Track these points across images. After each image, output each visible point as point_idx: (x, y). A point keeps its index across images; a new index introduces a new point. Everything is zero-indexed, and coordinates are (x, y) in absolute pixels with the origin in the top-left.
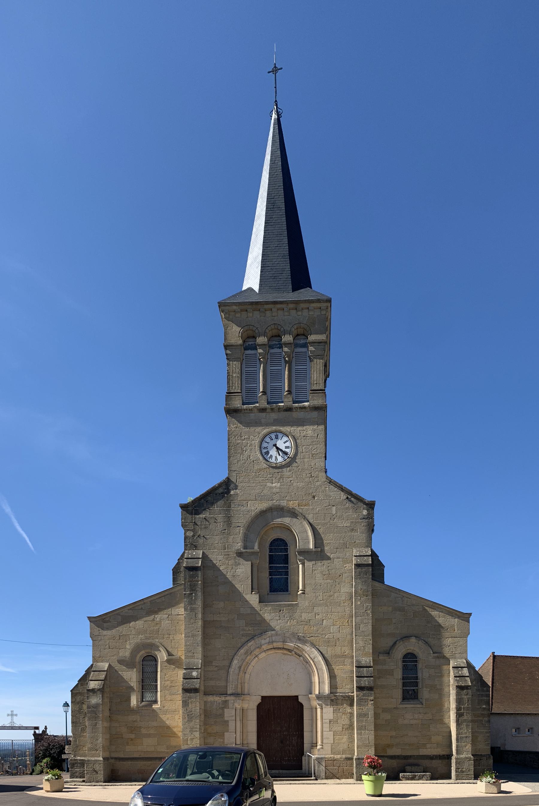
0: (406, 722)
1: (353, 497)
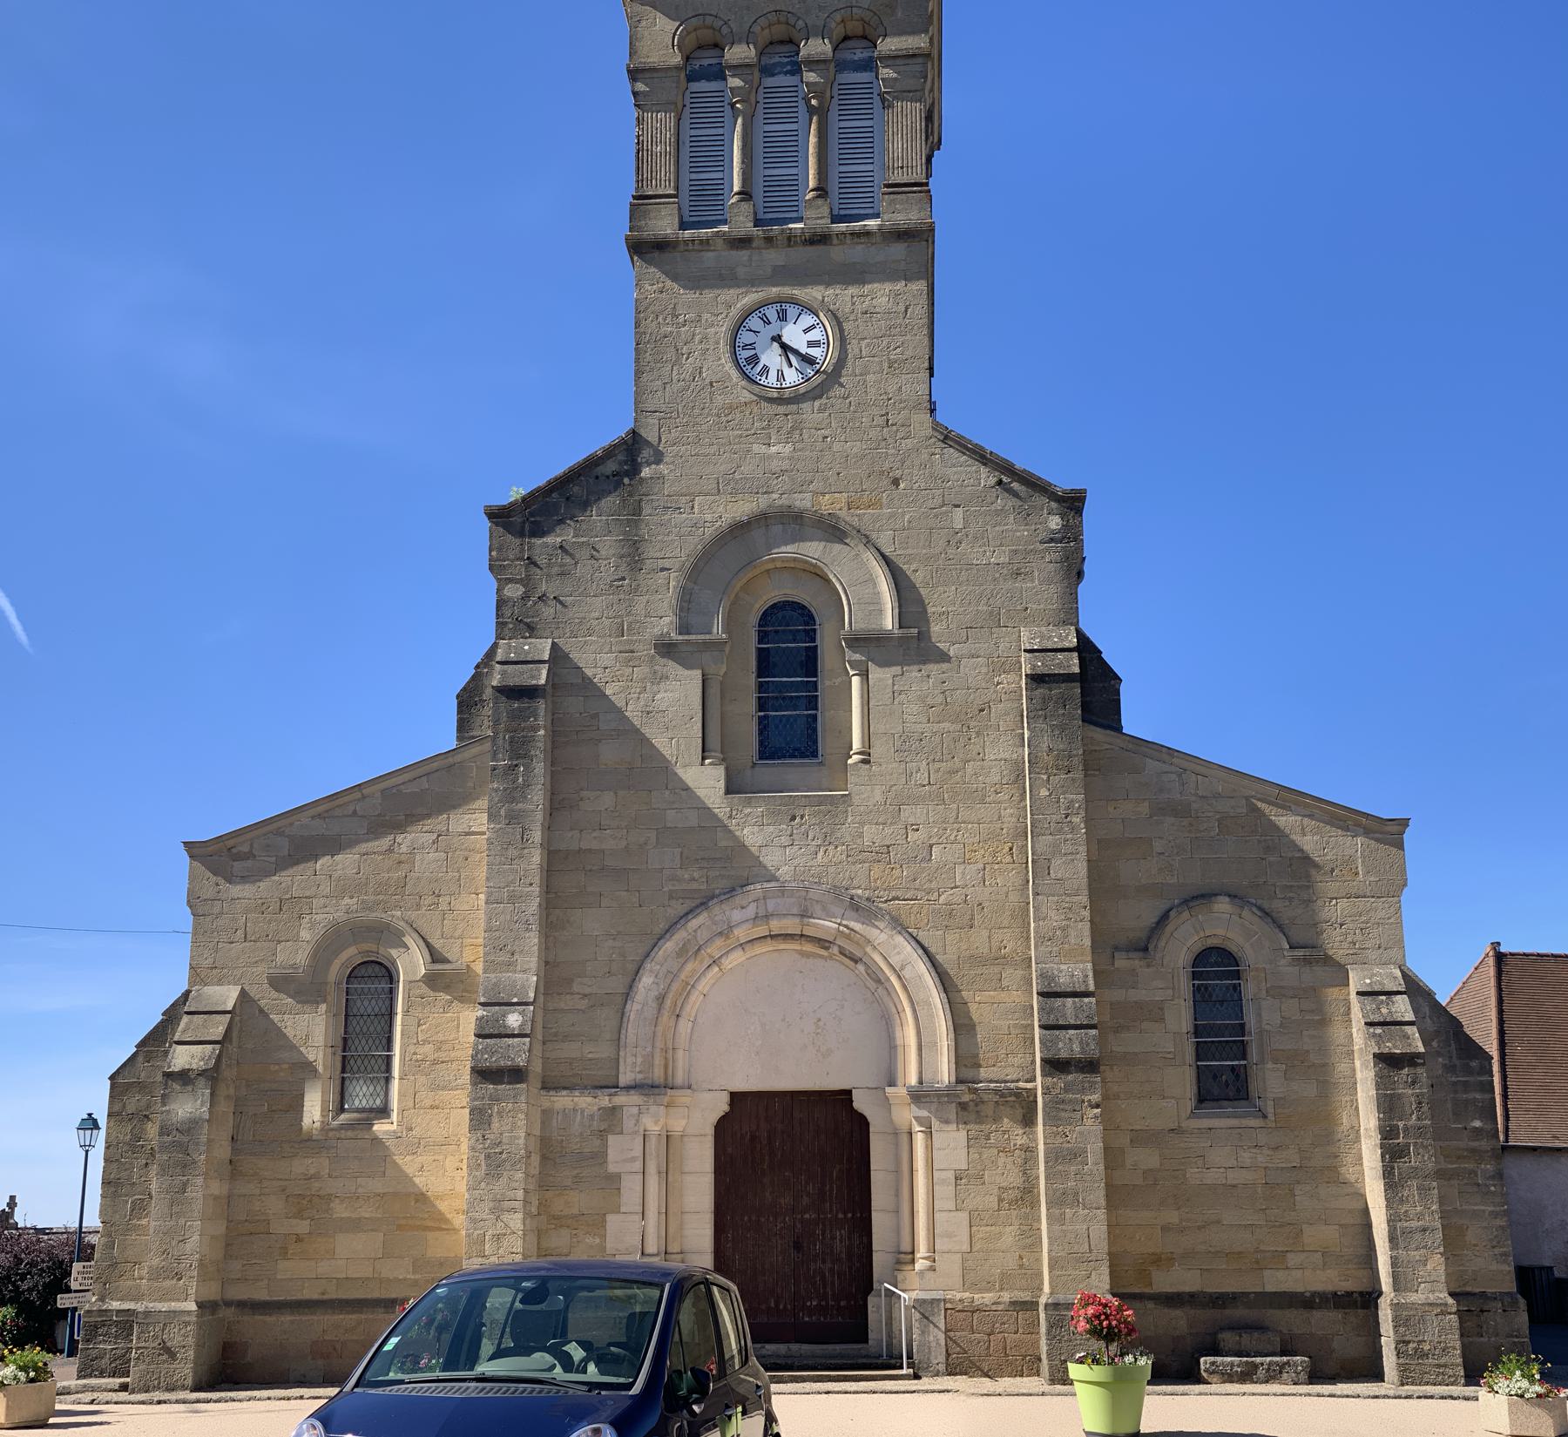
0: (1212, 1177)
1: (1017, 481)
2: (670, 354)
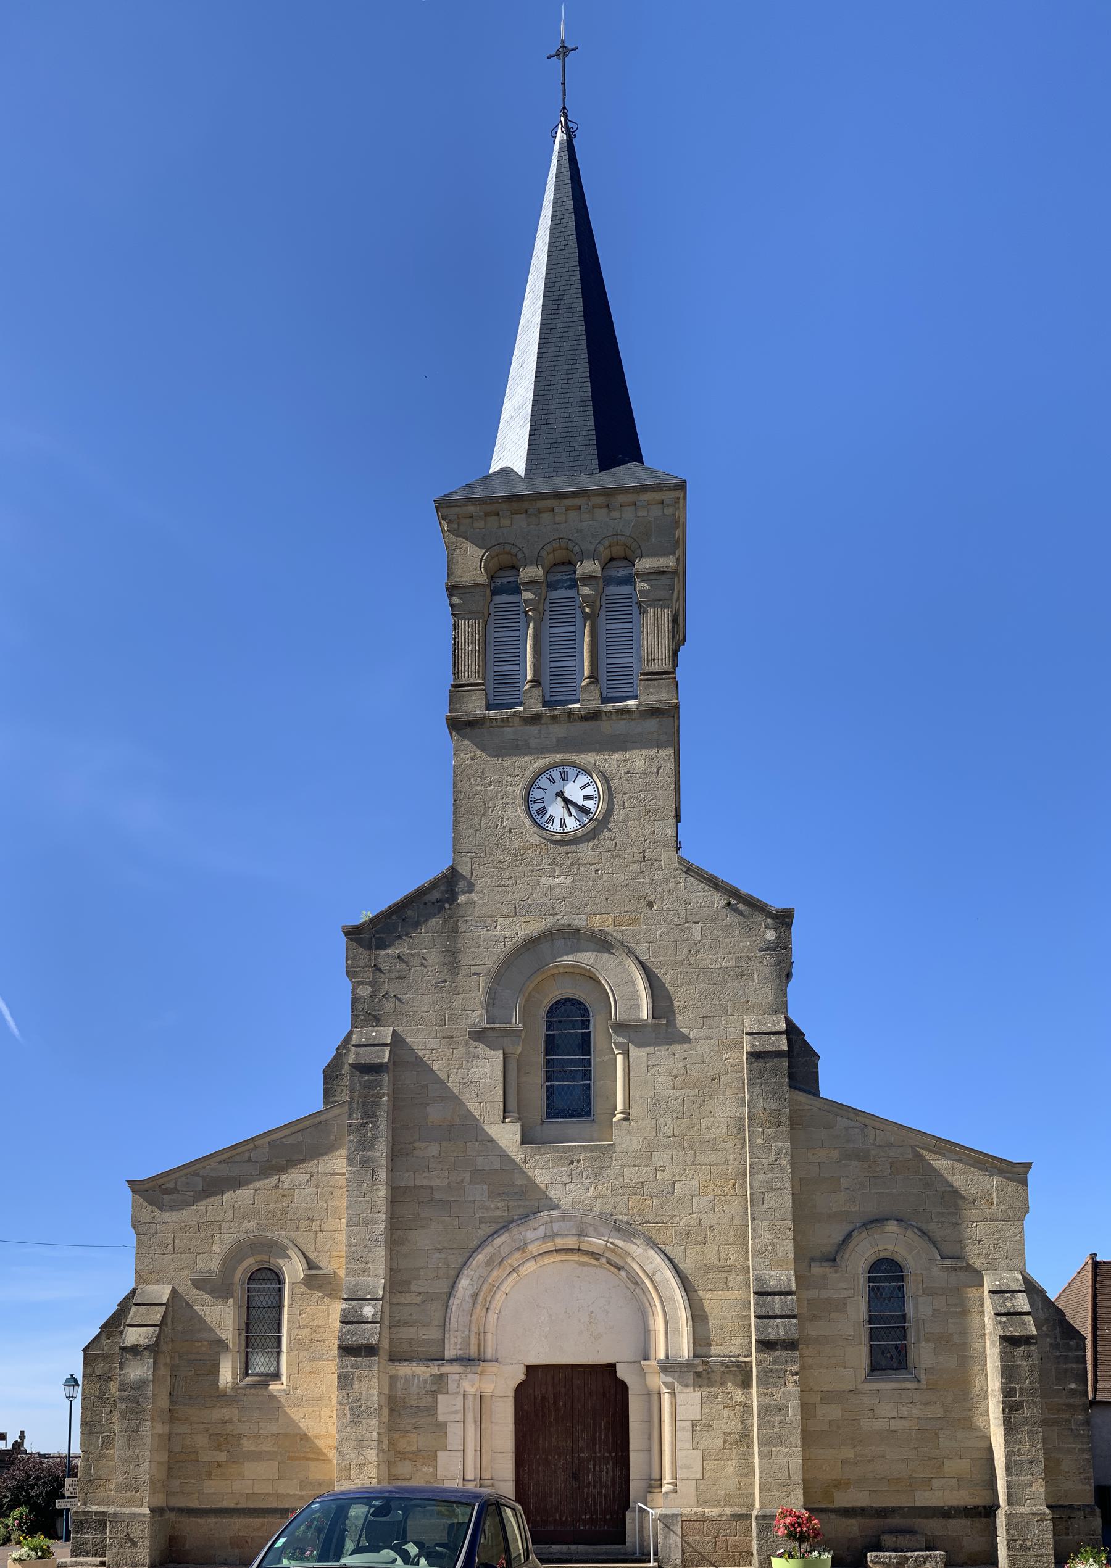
0: (878, 1425)
1: (740, 901)
2: (480, 808)
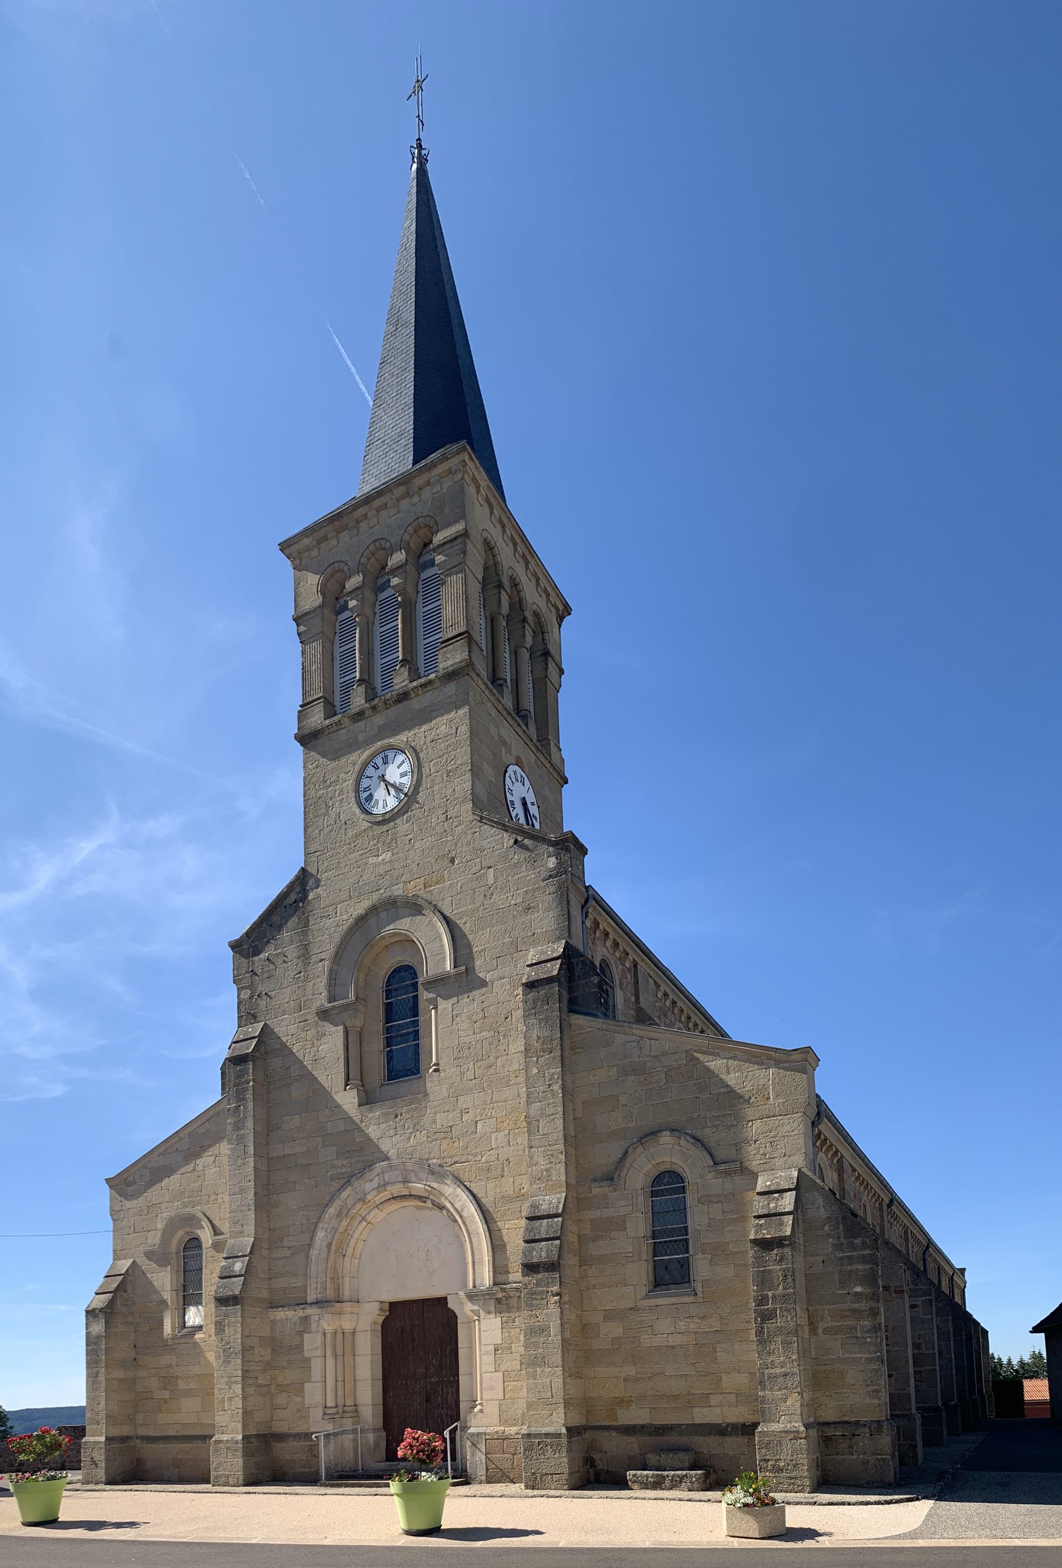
0: (658, 1341)
